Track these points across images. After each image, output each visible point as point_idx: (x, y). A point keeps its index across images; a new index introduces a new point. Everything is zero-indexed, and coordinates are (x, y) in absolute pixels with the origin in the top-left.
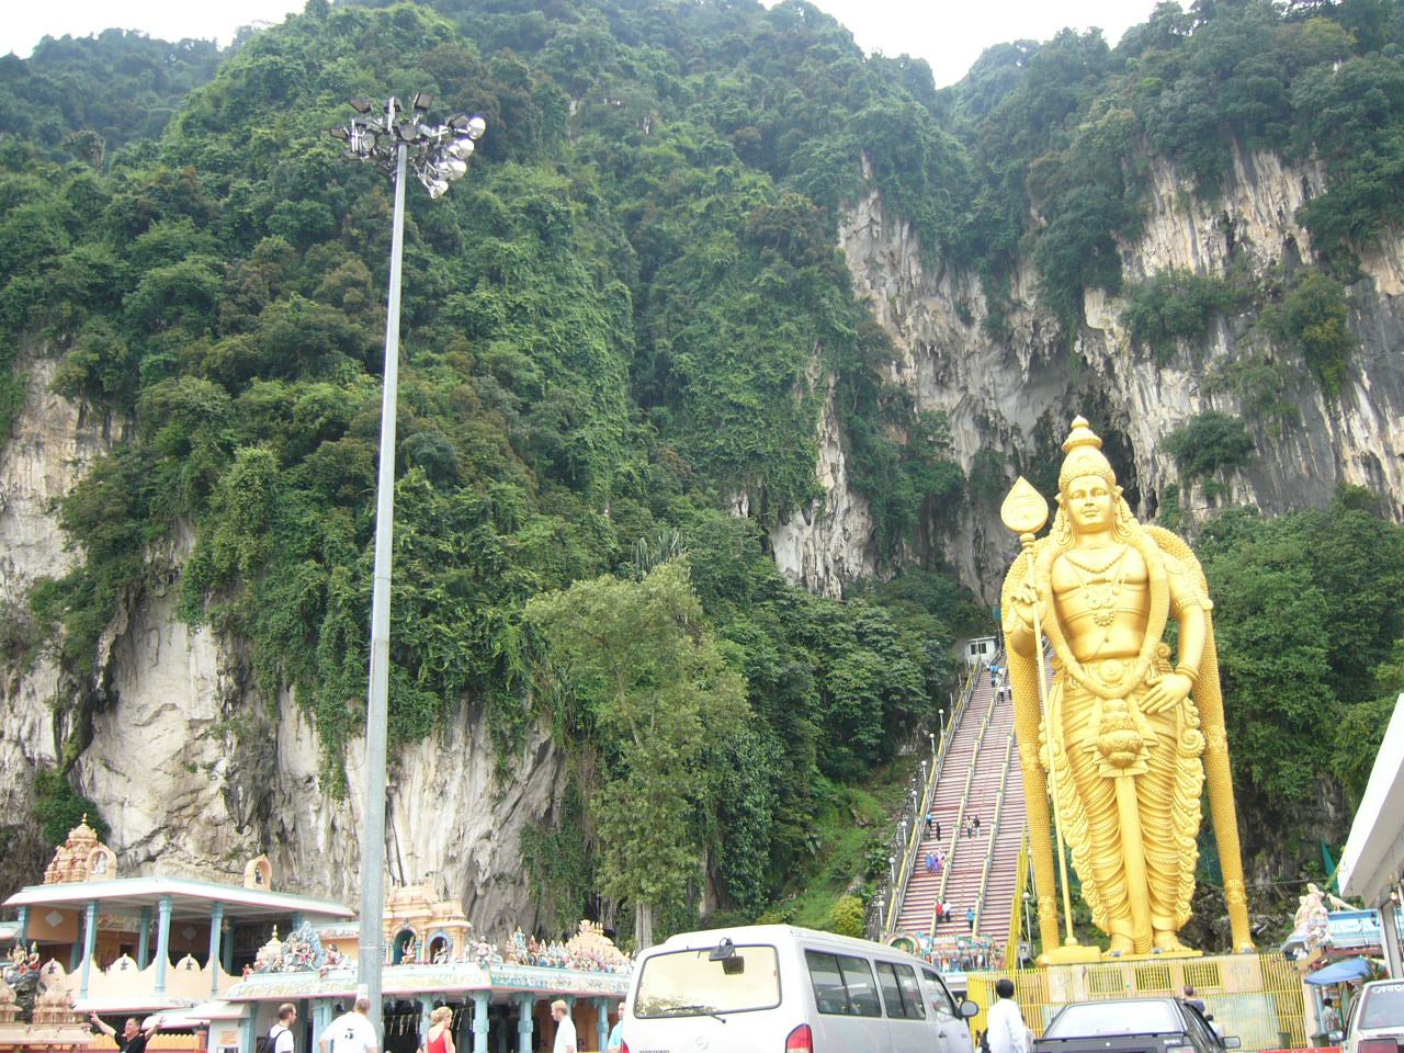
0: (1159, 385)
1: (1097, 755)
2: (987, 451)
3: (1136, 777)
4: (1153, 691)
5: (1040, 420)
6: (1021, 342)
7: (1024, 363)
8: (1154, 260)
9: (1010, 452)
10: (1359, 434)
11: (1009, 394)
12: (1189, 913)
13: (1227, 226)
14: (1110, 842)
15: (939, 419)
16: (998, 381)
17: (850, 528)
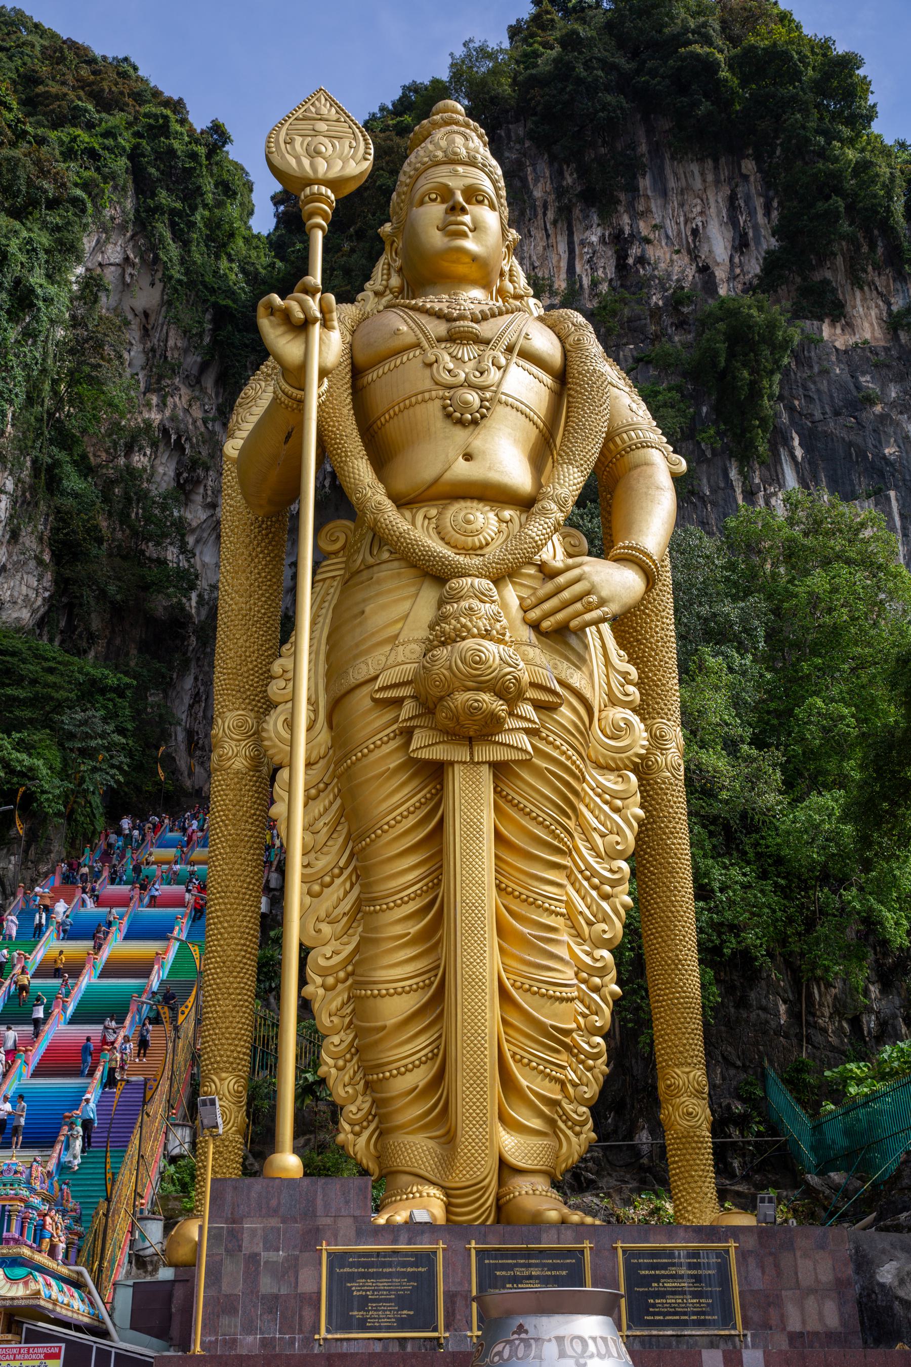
1: (408, 709)
3: (500, 770)
4: (561, 580)
12: (589, 1134)
13: (620, 242)
14: (414, 928)
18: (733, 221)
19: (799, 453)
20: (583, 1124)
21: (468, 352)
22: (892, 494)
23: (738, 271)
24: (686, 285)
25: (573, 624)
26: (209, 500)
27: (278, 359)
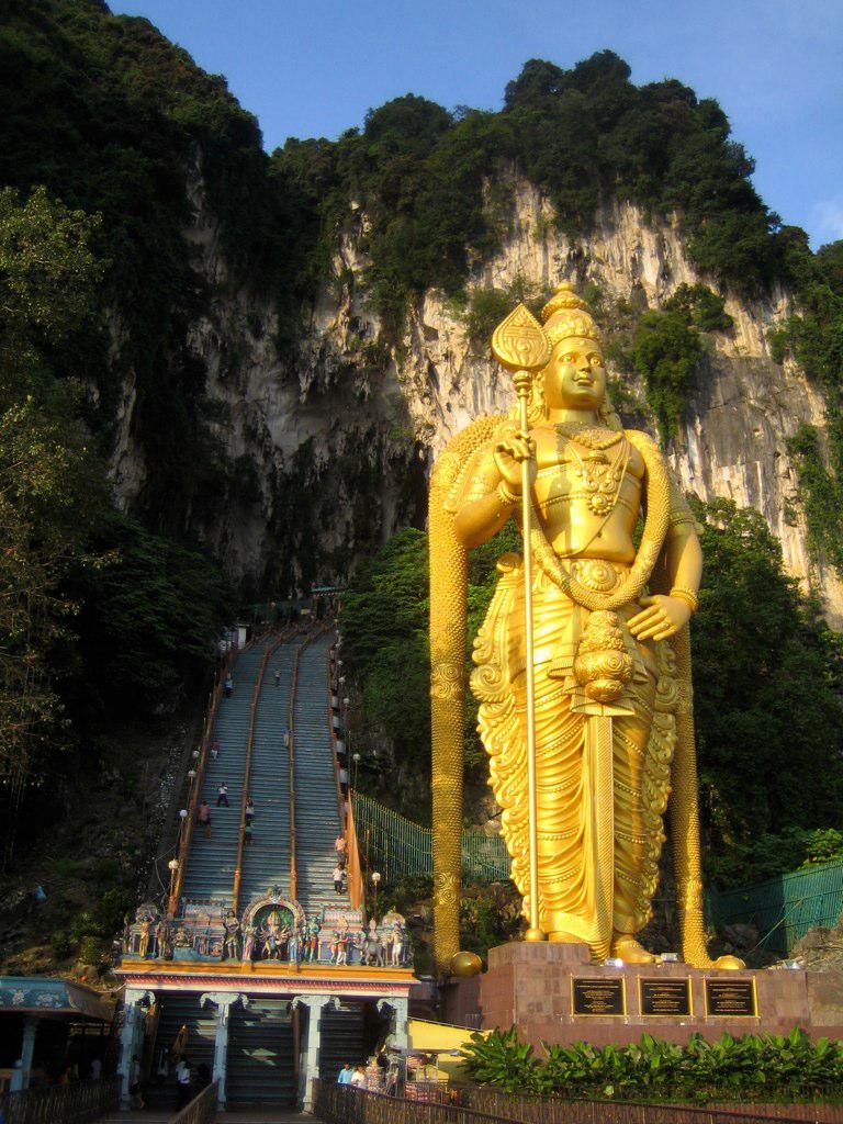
0: (494, 388)
1: (569, 683)
2: (247, 459)
4: (651, 609)
5: (301, 446)
6: (305, 365)
7: (304, 384)
8: (503, 275)
9: (268, 469)
10: (685, 473)
11: (281, 414)
12: (649, 913)
15: (220, 411)
16: (273, 399)
17: (124, 472)
18: (660, 256)
19: (699, 430)
20: (648, 908)
21: (601, 468)
22: (758, 463)
23: (661, 291)
24: (627, 298)
25: (655, 638)
26: (241, 389)
27: (507, 481)
